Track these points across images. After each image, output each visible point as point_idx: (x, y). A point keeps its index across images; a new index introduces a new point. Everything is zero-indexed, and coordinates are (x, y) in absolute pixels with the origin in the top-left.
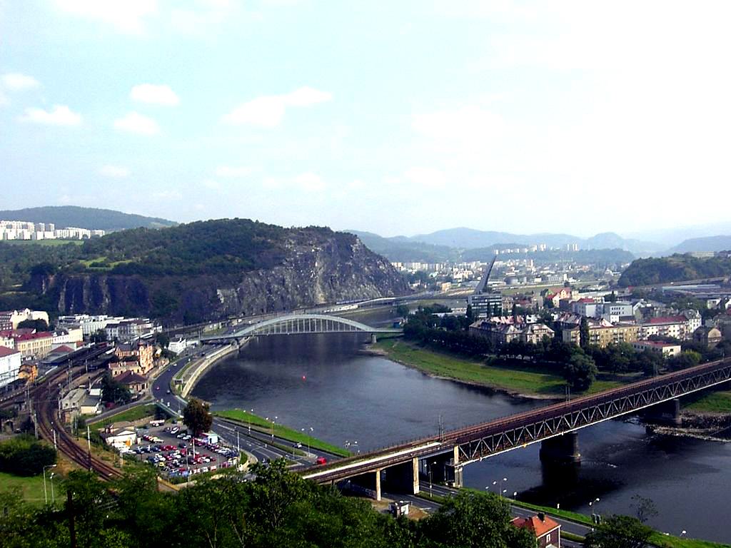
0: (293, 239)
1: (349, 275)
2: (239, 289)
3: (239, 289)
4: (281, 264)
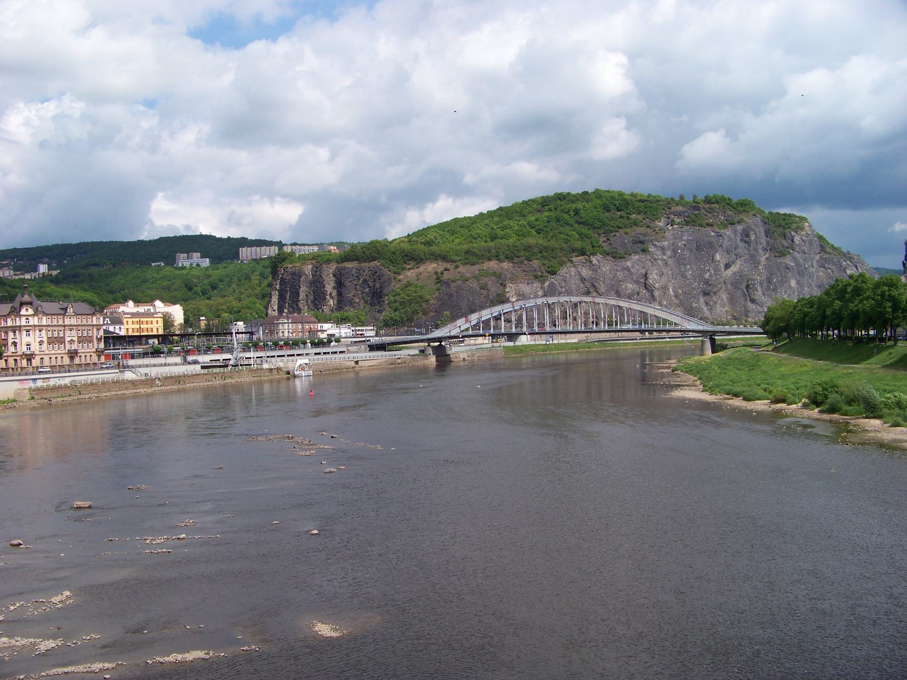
0: (679, 215)
2: (547, 284)
3: (547, 284)
4: (644, 251)
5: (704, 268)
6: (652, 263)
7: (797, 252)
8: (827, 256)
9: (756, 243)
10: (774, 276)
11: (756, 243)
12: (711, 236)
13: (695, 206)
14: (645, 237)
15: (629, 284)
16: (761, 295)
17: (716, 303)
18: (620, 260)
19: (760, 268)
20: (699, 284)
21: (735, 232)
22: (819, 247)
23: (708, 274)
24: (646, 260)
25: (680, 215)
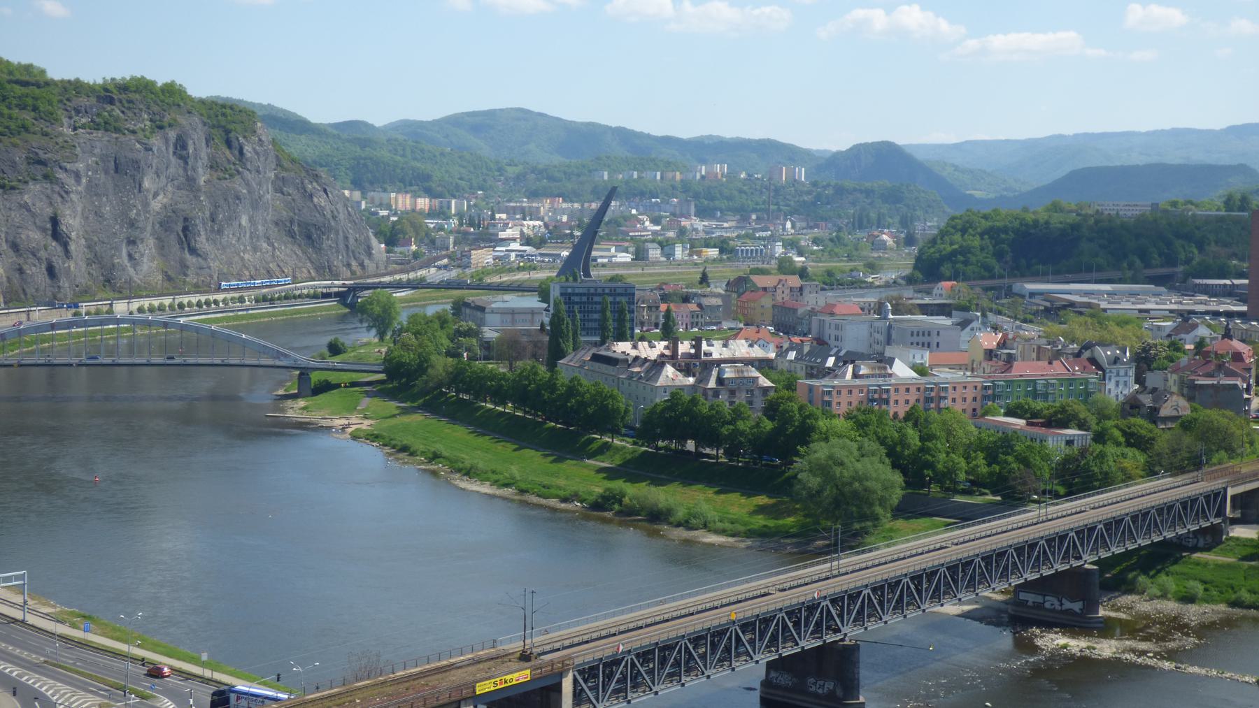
1: (232, 217)
5: (128, 201)
6: (62, 197)
7: (248, 170)
8: (284, 174)
9: (196, 158)
10: (220, 209)
11: (196, 158)
12: (137, 150)
13: (106, 96)
14: (46, 153)
15: (30, 233)
16: (204, 241)
17: (142, 255)
18: (13, 191)
19: (202, 198)
20: (122, 227)
21: (167, 140)
22: (274, 160)
23: (135, 211)
24: (53, 191)
25: (86, 112)
